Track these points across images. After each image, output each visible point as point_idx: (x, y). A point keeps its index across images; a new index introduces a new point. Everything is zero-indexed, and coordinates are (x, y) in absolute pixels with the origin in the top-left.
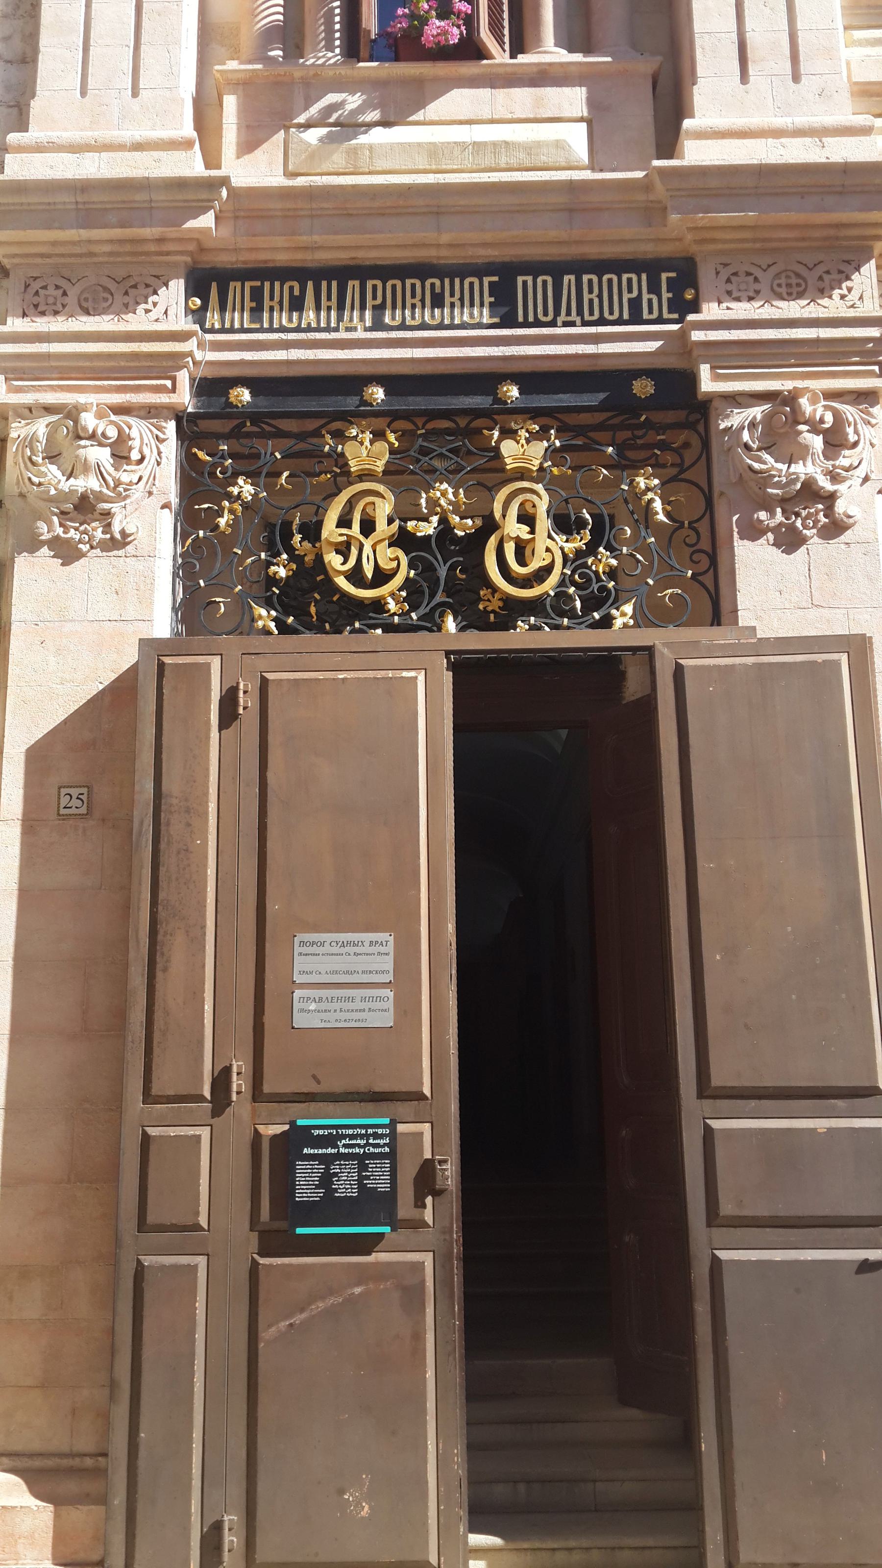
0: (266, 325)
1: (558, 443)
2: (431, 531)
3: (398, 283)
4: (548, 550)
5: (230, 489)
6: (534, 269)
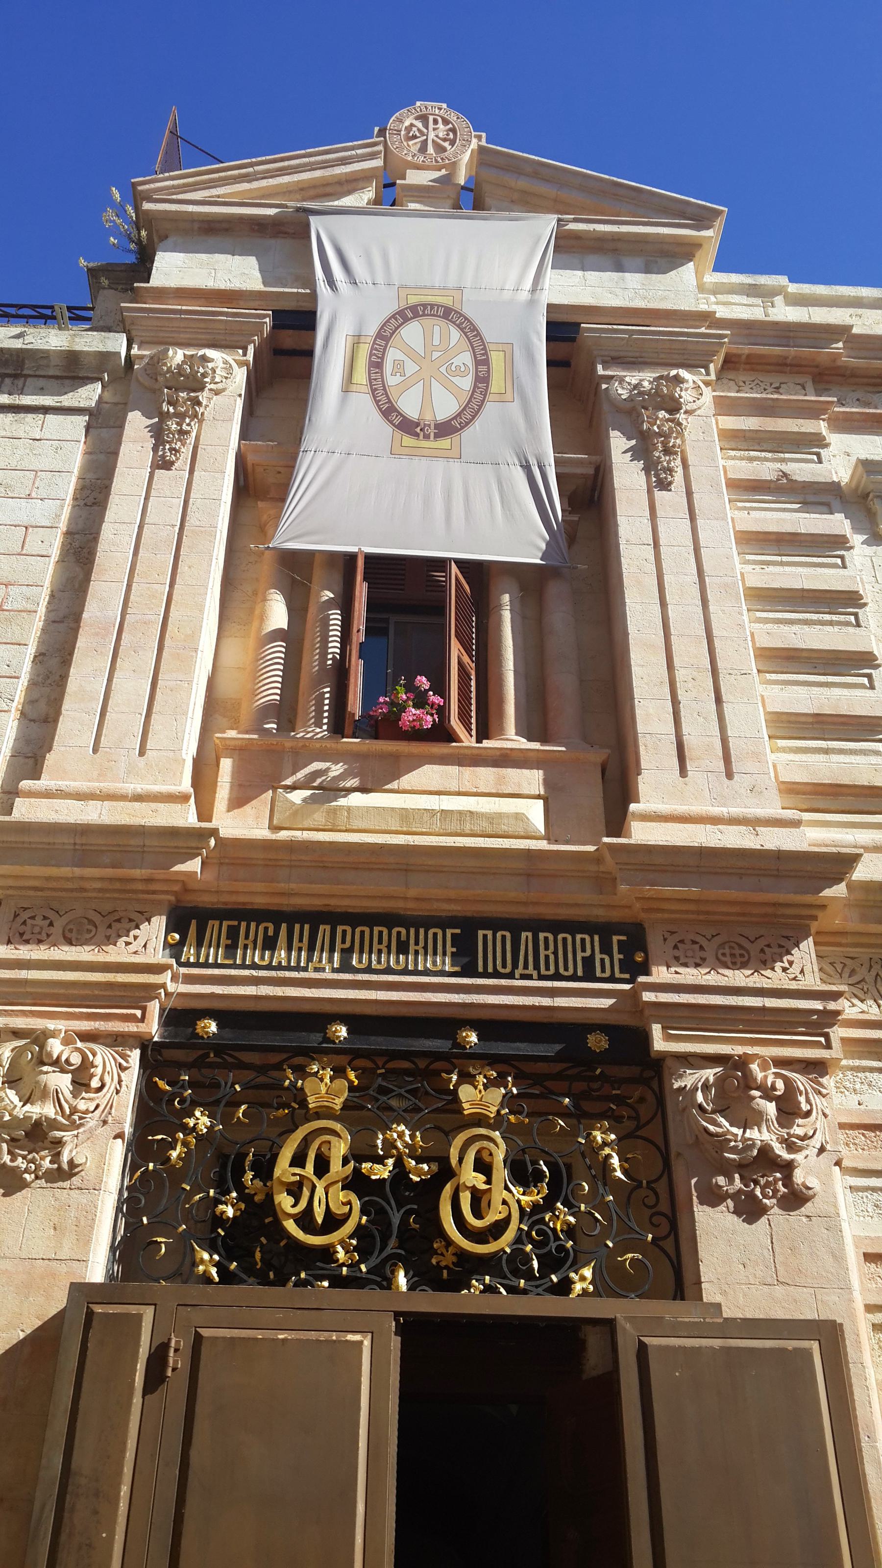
0: (238, 962)
1: (515, 1091)
2: (386, 1175)
3: (367, 930)
6: (495, 924)
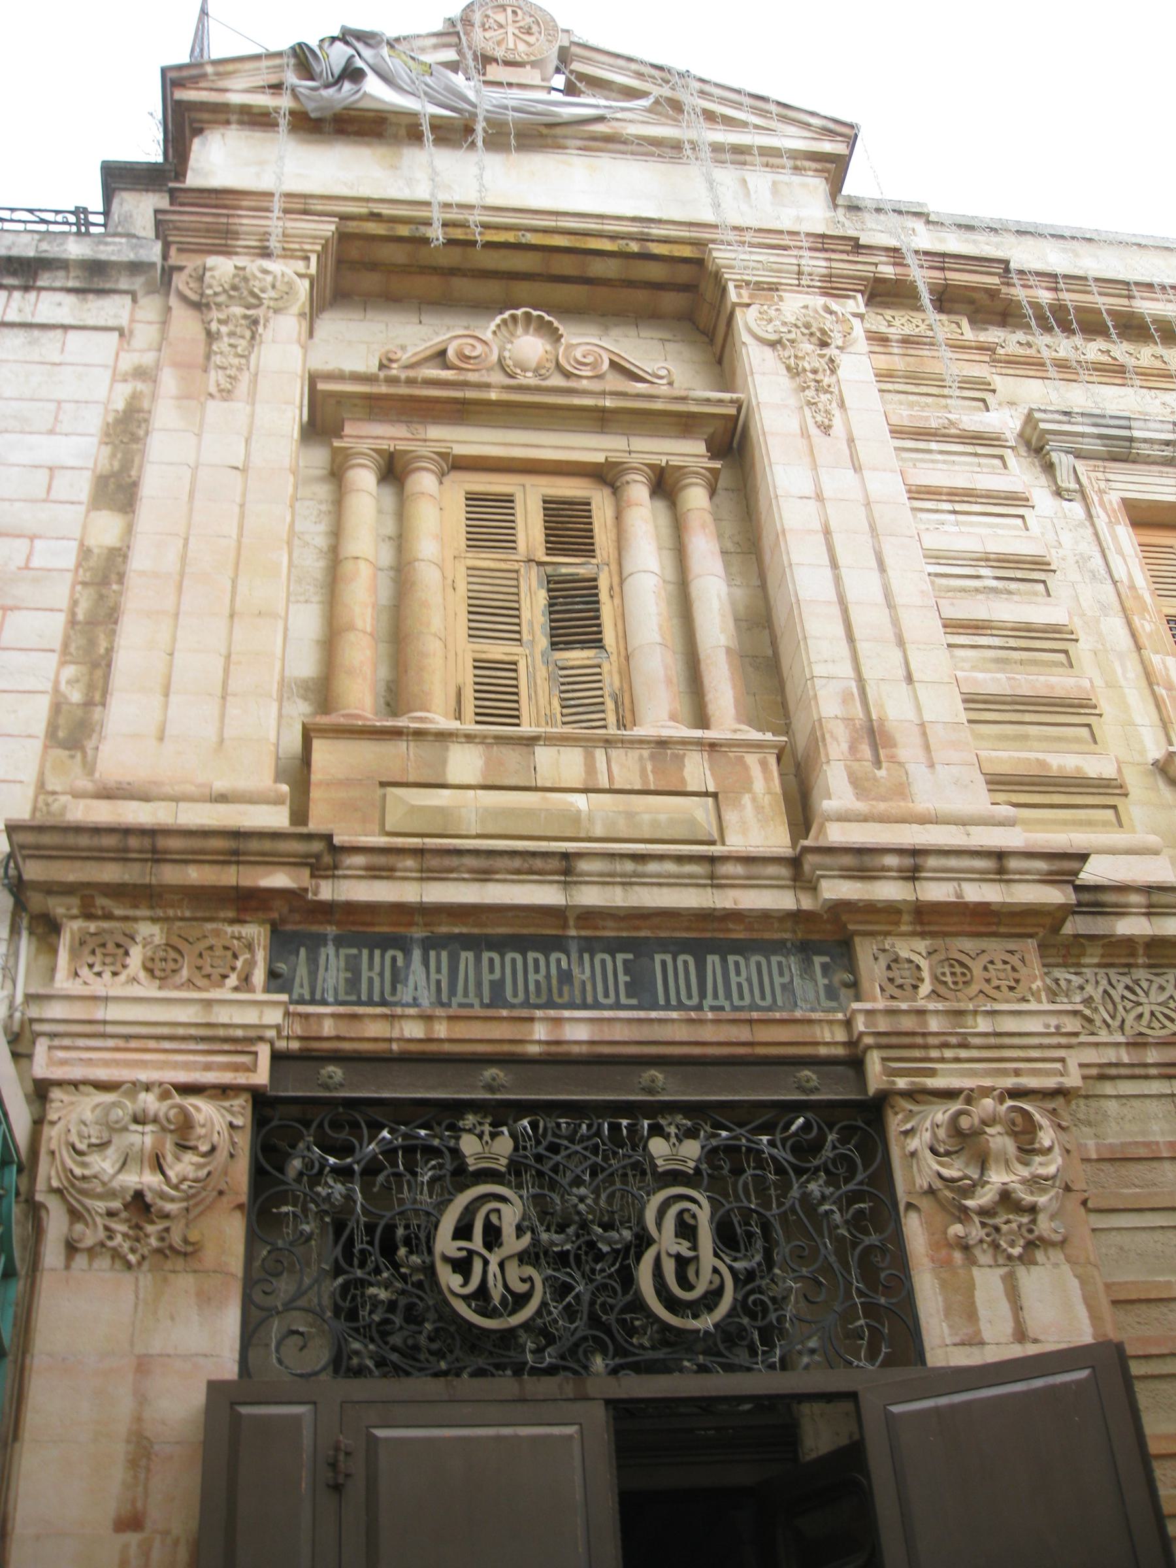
3: (519, 958)
4: (715, 1270)
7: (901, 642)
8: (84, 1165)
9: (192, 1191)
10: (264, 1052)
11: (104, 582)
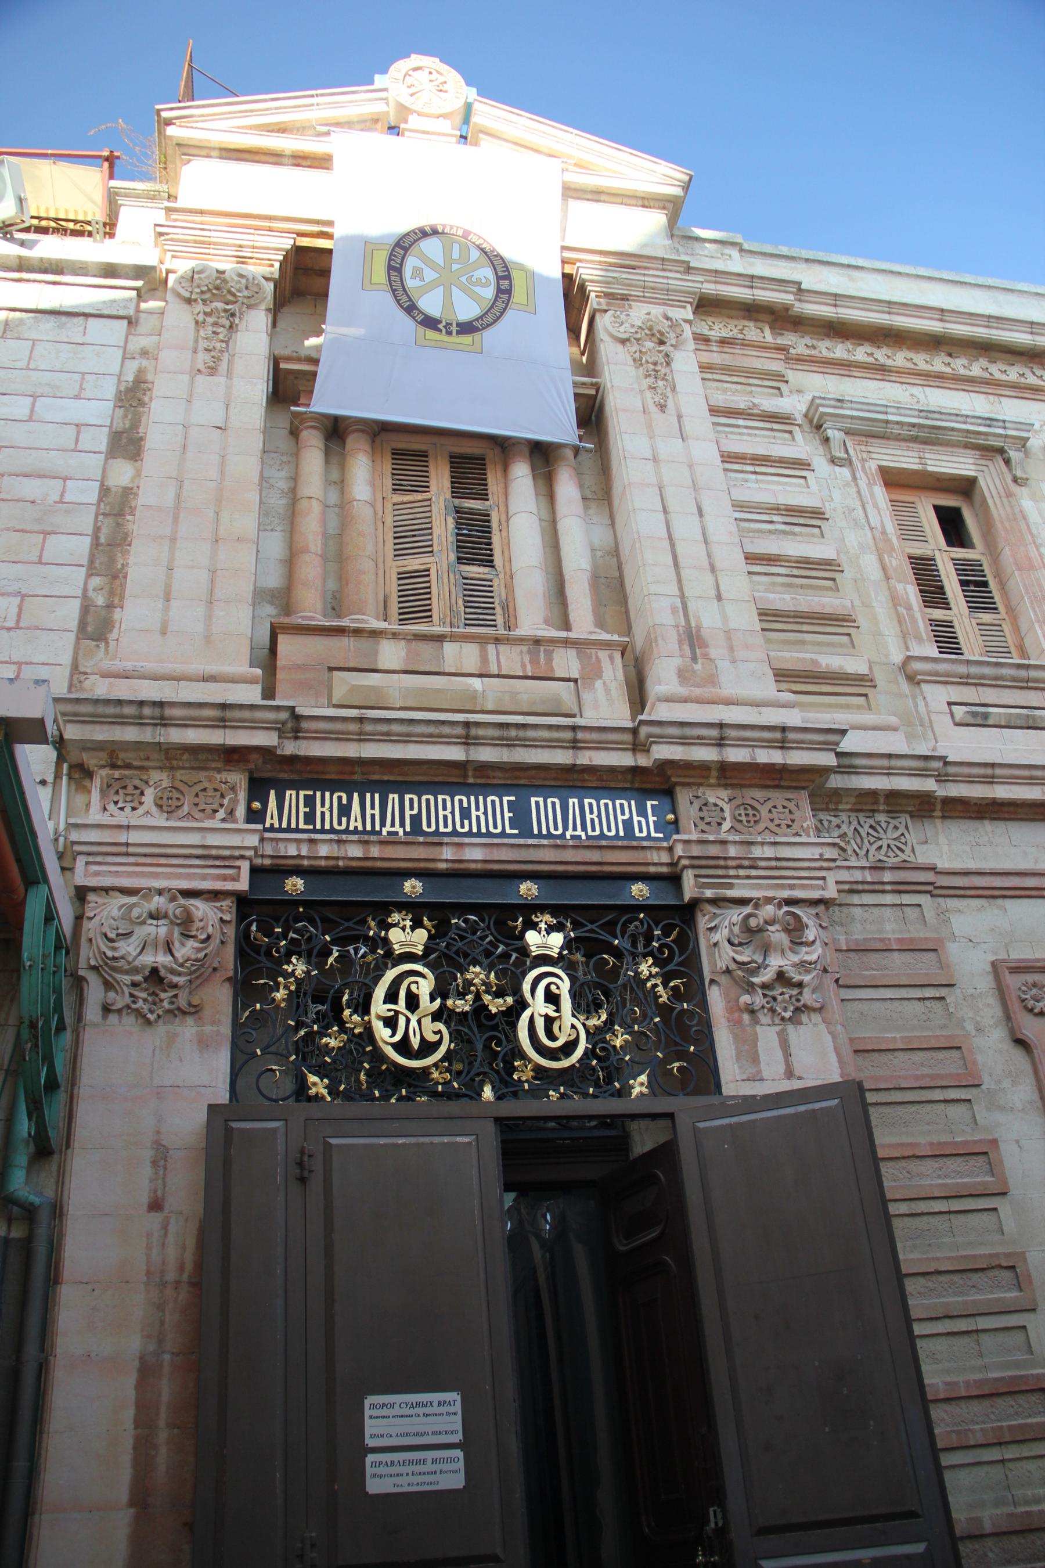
0: (318, 826)
1: (572, 935)
2: (467, 1008)
3: (432, 798)
4: (573, 1026)
5: (285, 967)
7: (713, 569)
8: (114, 949)
9: (193, 968)
10: (245, 866)
11: (121, 514)
